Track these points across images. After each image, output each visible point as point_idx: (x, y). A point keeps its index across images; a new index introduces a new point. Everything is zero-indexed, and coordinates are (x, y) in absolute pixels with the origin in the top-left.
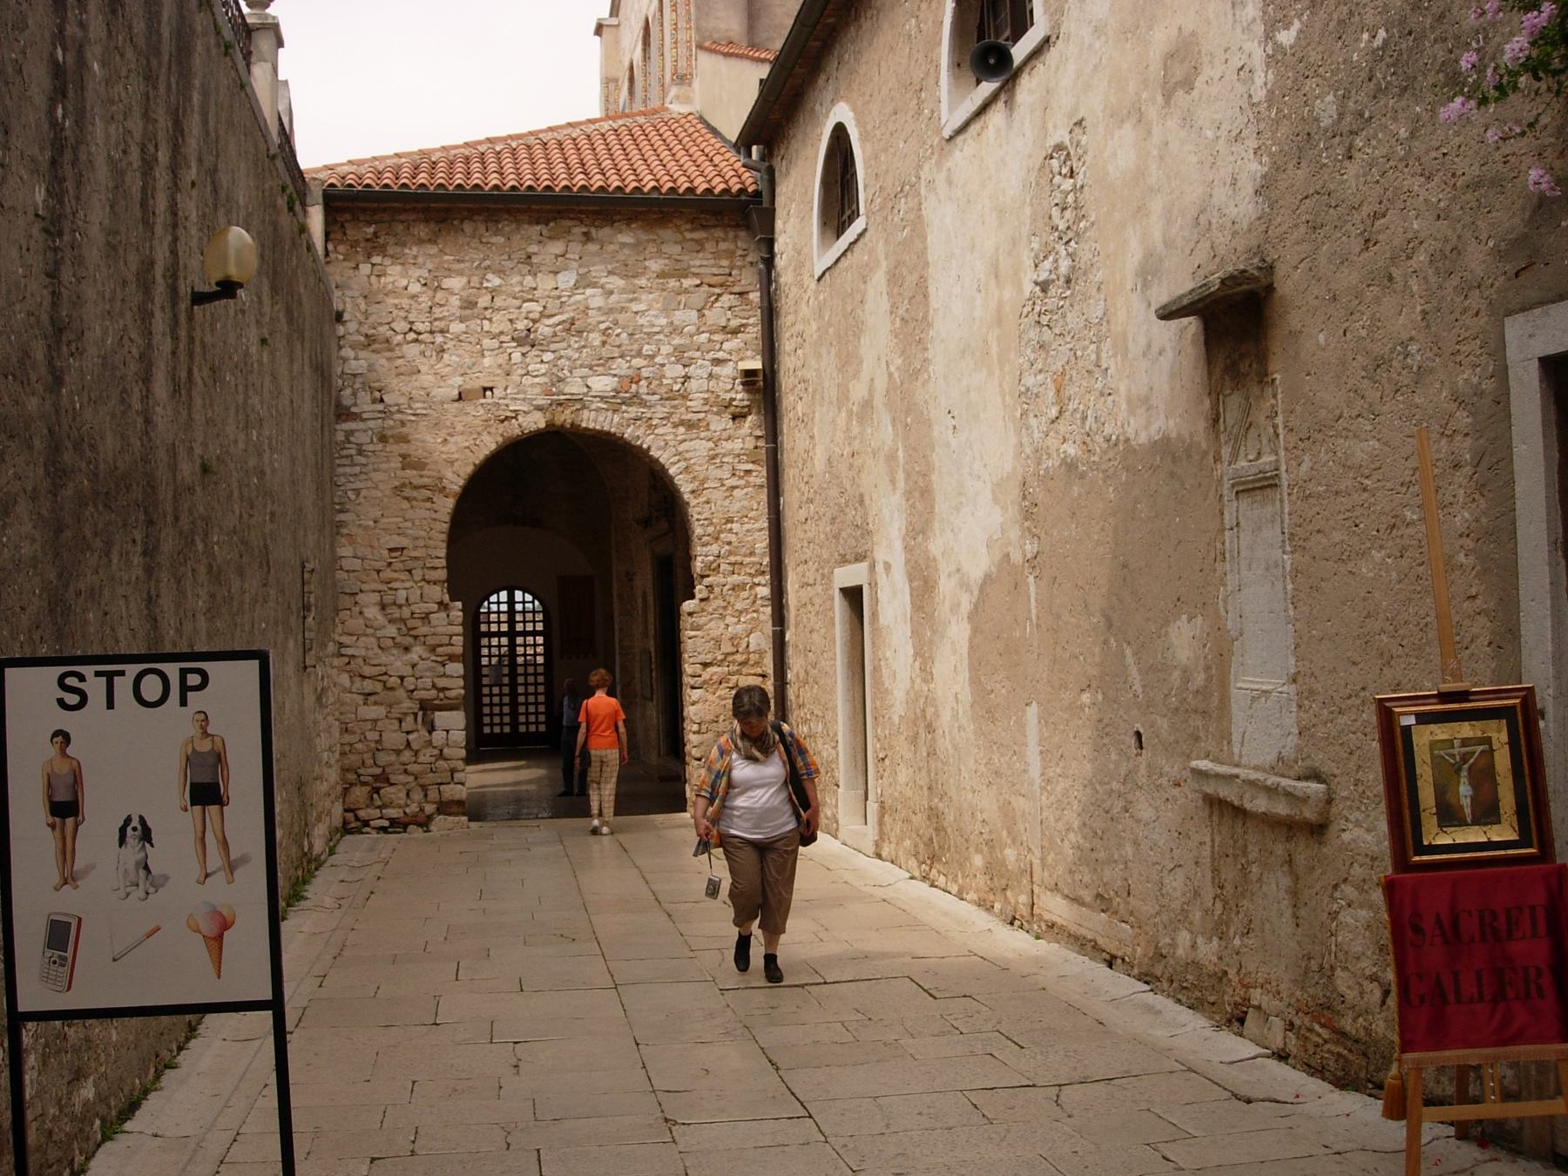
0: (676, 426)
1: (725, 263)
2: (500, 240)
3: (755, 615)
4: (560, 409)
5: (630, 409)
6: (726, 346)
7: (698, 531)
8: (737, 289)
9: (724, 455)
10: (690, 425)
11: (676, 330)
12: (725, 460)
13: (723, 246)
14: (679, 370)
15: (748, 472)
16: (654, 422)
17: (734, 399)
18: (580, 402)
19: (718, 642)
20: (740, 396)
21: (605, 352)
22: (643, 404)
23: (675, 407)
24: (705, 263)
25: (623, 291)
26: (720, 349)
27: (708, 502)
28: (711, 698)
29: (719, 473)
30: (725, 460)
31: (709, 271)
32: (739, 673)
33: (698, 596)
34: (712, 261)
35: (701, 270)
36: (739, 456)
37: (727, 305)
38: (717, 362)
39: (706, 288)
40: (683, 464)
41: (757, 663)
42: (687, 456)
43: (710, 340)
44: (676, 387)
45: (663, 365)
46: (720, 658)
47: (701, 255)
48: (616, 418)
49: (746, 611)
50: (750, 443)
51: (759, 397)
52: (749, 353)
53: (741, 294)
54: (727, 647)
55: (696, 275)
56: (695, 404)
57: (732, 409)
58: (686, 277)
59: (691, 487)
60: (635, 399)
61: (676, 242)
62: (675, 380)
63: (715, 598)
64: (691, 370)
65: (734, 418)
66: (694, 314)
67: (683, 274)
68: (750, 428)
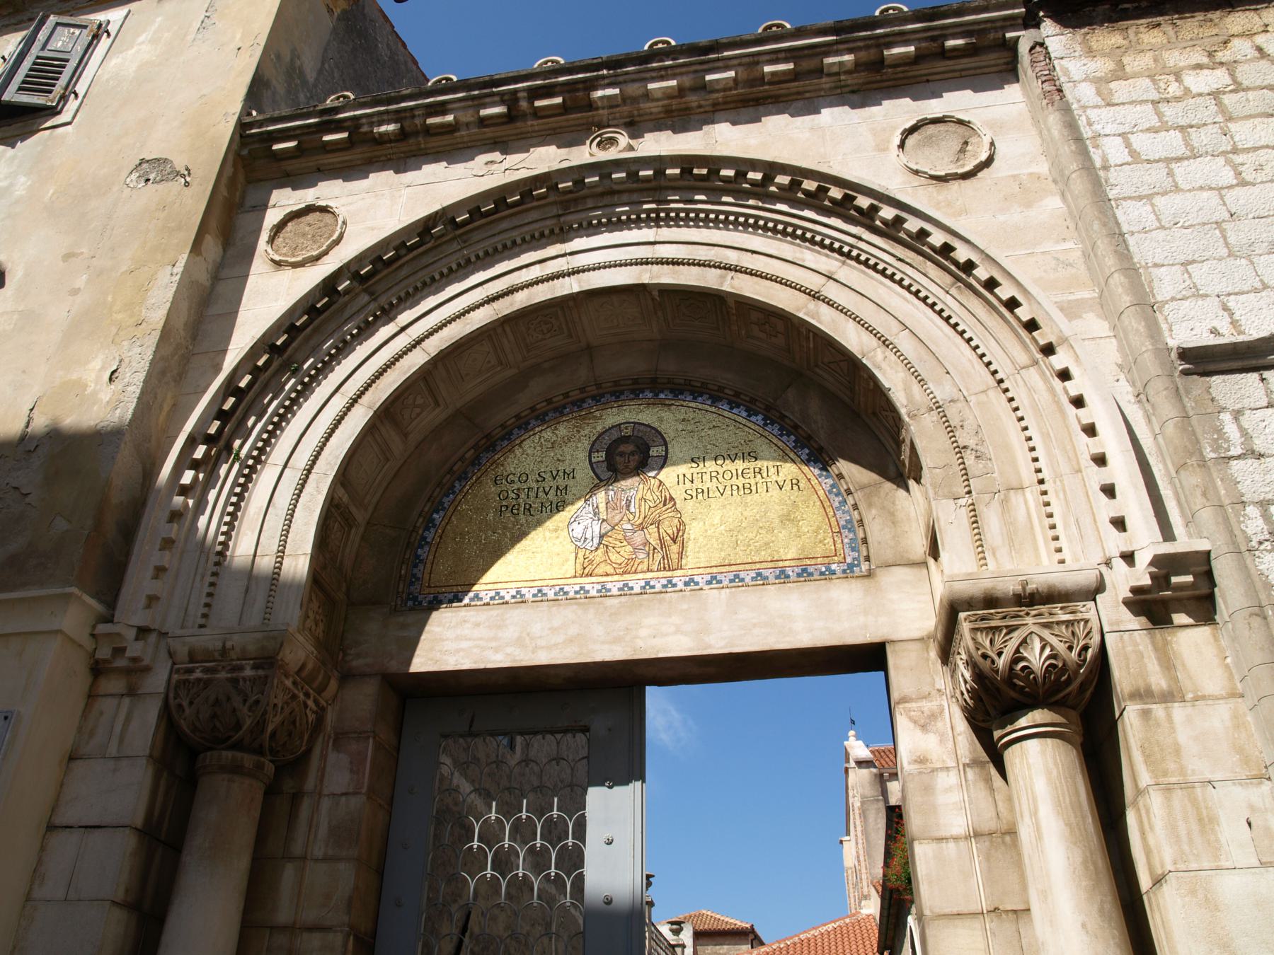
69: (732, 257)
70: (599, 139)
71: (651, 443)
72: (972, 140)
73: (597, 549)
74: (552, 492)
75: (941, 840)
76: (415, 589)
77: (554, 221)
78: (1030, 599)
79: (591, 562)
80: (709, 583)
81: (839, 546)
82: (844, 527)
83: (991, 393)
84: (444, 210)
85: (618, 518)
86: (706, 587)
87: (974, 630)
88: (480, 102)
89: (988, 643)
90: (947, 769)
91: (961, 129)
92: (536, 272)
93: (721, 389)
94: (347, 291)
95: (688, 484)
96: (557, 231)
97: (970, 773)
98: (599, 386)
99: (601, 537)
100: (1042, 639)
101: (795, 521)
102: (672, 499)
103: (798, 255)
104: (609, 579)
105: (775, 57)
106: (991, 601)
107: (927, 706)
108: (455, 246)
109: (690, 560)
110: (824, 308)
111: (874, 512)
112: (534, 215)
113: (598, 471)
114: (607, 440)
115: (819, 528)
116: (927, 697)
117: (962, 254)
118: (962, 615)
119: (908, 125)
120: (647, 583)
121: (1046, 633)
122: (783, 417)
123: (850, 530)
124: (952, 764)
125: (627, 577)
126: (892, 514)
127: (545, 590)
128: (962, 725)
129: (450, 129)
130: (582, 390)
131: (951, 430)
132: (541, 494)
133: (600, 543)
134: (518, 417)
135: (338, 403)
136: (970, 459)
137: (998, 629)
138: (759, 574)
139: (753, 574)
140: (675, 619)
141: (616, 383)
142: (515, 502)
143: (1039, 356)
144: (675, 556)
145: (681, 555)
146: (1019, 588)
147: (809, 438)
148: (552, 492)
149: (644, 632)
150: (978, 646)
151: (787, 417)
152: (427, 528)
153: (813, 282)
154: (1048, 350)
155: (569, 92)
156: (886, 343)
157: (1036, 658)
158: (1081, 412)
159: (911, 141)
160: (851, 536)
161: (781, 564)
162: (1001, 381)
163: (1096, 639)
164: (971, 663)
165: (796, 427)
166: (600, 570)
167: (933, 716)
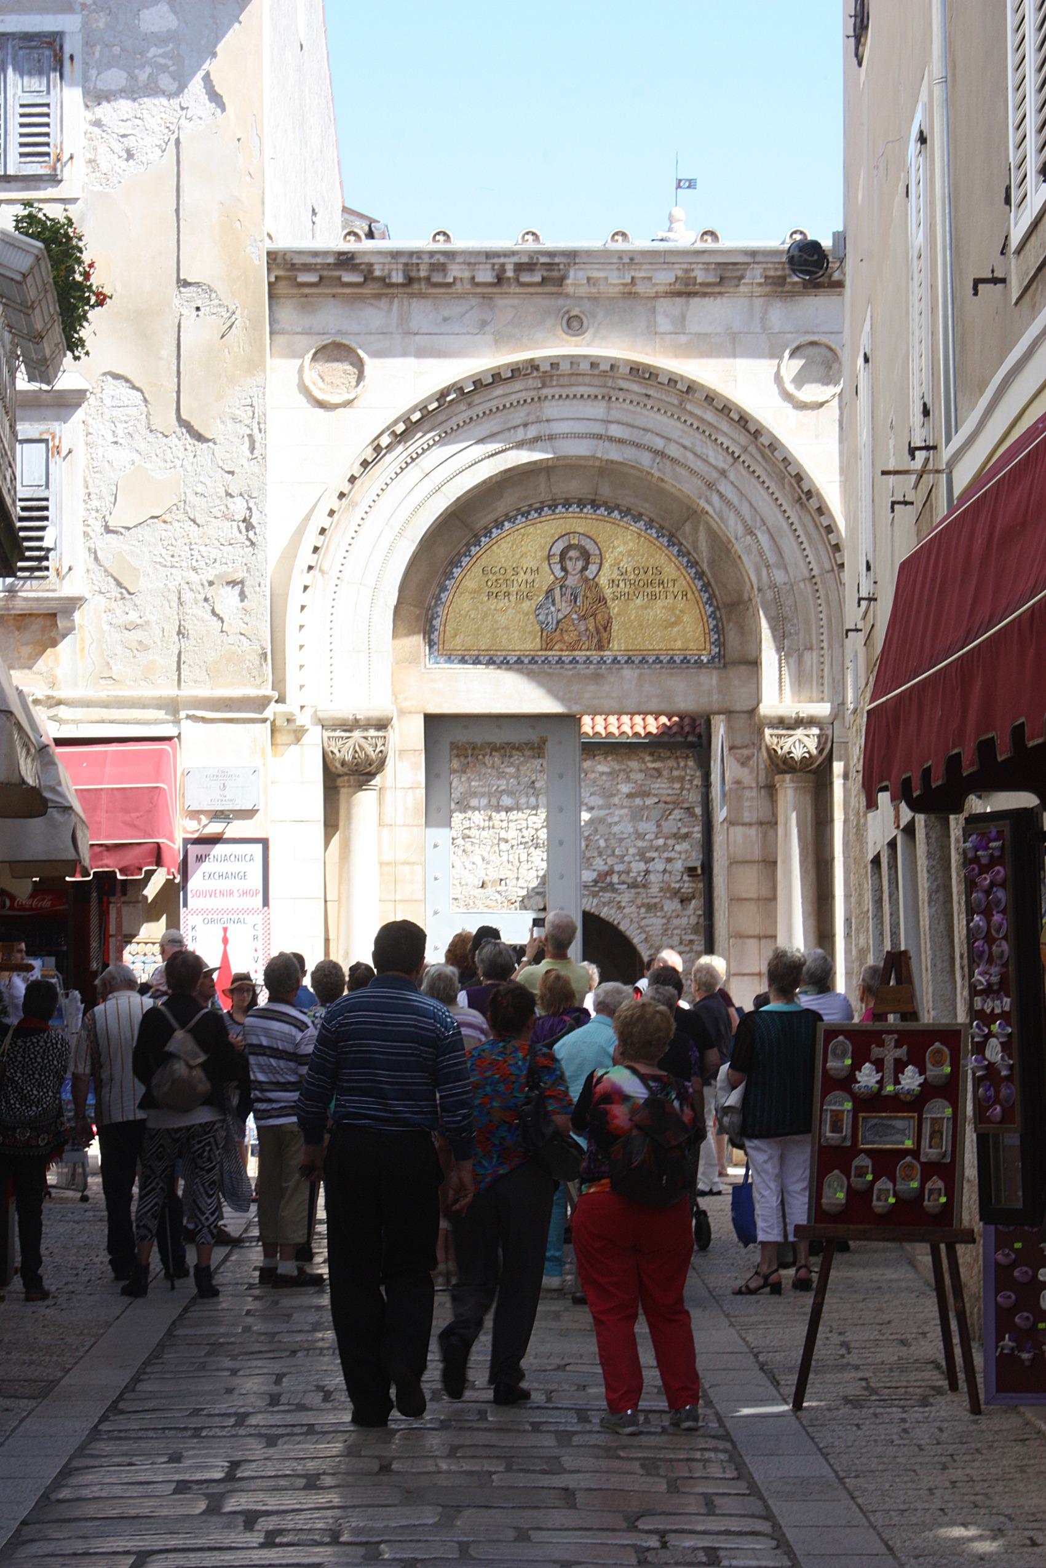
0: (639, 907)
1: (677, 786)
2: (512, 770)
5: (607, 895)
6: (677, 848)
8: (686, 805)
10: (650, 908)
11: (641, 836)
13: (675, 773)
14: (642, 866)
15: (691, 942)
16: (623, 904)
20: (688, 886)
22: (615, 890)
23: (638, 893)
25: (601, 808)
30: (675, 932)
31: (665, 792)
34: (667, 785)
35: (661, 791)
37: (678, 817)
38: (669, 860)
39: (662, 805)
40: (643, 936)
44: (639, 879)
45: (630, 862)
48: (595, 901)
50: (693, 920)
51: (701, 885)
53: (688, 809)
56: (654, 890)
60: (611, 887)
61: (641, 771)
62: (639, 872)
65: (682, 901)
67: (645, 794)
68: (695, 910)
69: (659, 444)
71: (591, 552)
72: (835, 366)
79: (551, 640)
85: (569, 609)
87: (771, 736)
91: (829, 355)
93: (641, 515)
95: (615, 588)
96: (536, 399)
97: (763, 791)
99: (558, 622)
102: (604, 598)
103: (704, 451)
104: (564, 653)
107: (746, 752)
108: (463, 407)
109: (615, 645)
111: (731, 625)
112: (518, 385)
116: (746, 747)
121: (805, 739)
124: (754, 785)
125: (576, 653)
126: (742, 627)
127: (523, 658)
129: (449, 285)
130: (542, 502)
134: (496, 520)
138: (657, 658)
140: (606, 688)
141: (567, 499)
143: (835, 568)
147: (697, 563)
149: (587, 695)
151: (681, 544)
152: (436, 605)
155: (547, 270)
161: (671, 652)
162: (814, 577)
163: (829, 745)
165: (689, 553)
167: (749, 758)
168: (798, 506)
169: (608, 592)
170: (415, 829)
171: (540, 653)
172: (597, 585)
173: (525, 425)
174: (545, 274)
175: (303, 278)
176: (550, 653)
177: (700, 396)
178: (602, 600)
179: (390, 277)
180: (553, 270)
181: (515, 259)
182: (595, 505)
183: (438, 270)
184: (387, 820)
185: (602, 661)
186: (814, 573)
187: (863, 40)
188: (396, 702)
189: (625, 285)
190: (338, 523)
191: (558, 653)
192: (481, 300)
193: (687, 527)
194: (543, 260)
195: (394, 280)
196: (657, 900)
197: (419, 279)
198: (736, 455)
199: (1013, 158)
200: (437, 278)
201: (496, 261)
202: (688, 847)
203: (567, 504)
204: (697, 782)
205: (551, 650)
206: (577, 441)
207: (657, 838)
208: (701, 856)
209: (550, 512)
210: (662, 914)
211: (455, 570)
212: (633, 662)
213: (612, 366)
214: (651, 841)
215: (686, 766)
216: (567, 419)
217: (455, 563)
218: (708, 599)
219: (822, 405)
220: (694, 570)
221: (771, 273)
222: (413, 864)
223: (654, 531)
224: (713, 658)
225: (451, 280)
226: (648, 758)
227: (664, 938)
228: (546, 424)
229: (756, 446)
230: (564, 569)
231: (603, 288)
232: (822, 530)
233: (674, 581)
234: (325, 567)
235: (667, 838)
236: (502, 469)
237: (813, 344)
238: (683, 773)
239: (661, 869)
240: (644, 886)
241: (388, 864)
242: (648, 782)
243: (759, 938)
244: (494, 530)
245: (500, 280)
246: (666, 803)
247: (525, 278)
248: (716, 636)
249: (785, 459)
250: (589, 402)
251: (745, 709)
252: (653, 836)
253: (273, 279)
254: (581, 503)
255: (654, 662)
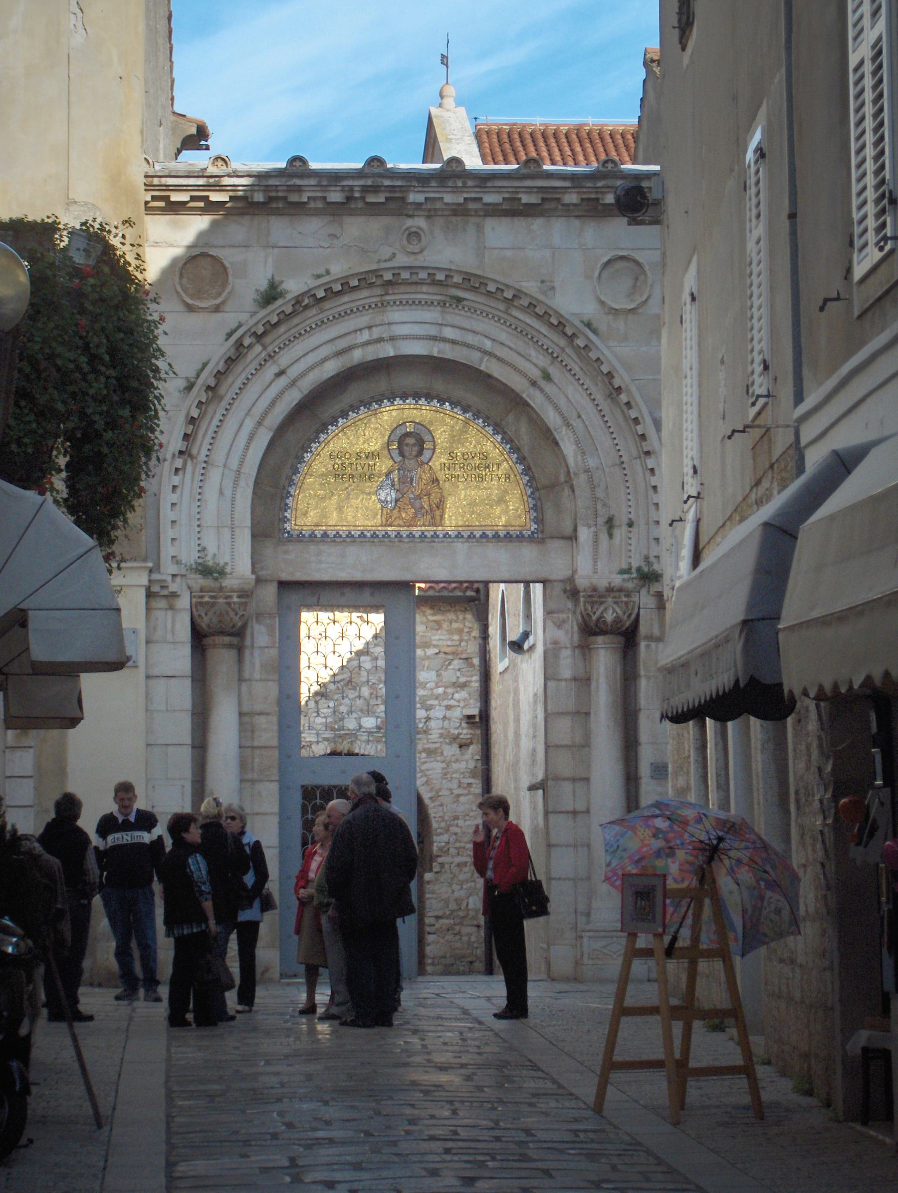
1: (456, 637)
3: (473, 884)
4: (340, 740)
6: (456, 696)
7: (435, 825)
8: (464, 656)
9: (453, 773)
12: (454, 776)
13: (455, 625)
15: (469, 784)
17: (461, 734)
18: (353, 736)
19: (447, 902)
20: (466, 732)
21: (373, 702)
24: (442, 637)
26: (452, 698)
27: (441, 805)
28: (442, 941)
29: (450, 785)
30: (454, 776)
31: (445, 643)
32: (461, 924)
33: (434, 870)
34: (448, 637)
35: (440, 643)
36: (463, 773)
37: (458, 667)
38: (449, 708)
39: (442, 655)
40: (424, 779)
41: (474, 918)
42: (428, 773)
43: (445, 692)
46: (448, 913)
47: (439, 632)
49: (467, 881)
50: (472, 764)
51: (478, 732)
52: (472, 701)
54: (453, 906)
55: (435, 646)
56: (434, 736)
57: (458, 741)
58: (429, 647)
59: (430, 795)
63: (446, 872)
64: (432, 714)
65: (461, 747)
66: (434, 673)
68: (472, 754)
69: (488, 345)
70: (407, 232)
72: (642, 278)
73: (394, 508)
74: (366, 467)
75: (559, 680)
76: (287, 526)
77: (378, 299)
78: (610, 590)
79: (391, 517)
80: (457, 537)
81: (528, 520)
82: (532, 509)
83: (617, 468)
84: (310, 290)
85: (406, 490)
86: (455, 540)
87: (585, 602)
88: (324, 188)
89: (590, 608)
90: (566, 648)
92: (365, 336)
94: (249, 346)
96: (380, 305)
97: (577, 650)
98: (393, 393)
99: (396, 501)
100: (613, 609)
101: (506, 502)
102: (437, 480)
105: (529, 190)
106: (595, 589)
107: (563, 616)
108: (314, 311)
110: (537, 394)
112: (365, 293)
113: (393, 455)
114: (399, 433)
115: (518, 508)
116: (562, 612)
117: (617, 382)
118: (581, 594)
119: (605, 259)
120: (423, 533)
121: (615, 606)
122: (505, 433)
123: (535, 511)
124: (569, 645)
128: (576, 628)
131: (593, 488)
132: (359, 468)
133: (396, 505)
134: (342, 411)
135: (249, 424)
136: (599, 506)
137: (596, 602)
138: (484, 533)
139: (481, 533)
142: (343, 472)
143: (642, 455)
144: (438, 518)
145: (442, 517)
146: (607, 585)
148: (366, 467)
150: (586, 610)
152: (290, 486)
153: (535, 373)
154: (648, 453)
155: (390, 192)
156: (568, 425)
157: (609, 617)
158: (654, 496)
159: (605, 274)
160: (535, 514)
161: (496, 528)
163: (636, 610)
164: (581, 613)
165: (512, 441)
166: (396, 523)
167: (564, 621)
168: (609, 400)
169: (441, 476)
170: (270, 683)
171: (380, 528)
172: (431, 467)
173: (370, 328)
174: (388, 195)
175: (175, 197)
176: (389, 528)
177: (525, 302)
178: (436, 481)
179: (252, 198)
180: (395, 192)
181: (361, 182)
182: (429, 397)
183: (295, 191)
184: (246, 675)
185: (435, 536)
186: (623, 459)
187: (687, 32)
188: (253, 572)
189: (459, 204)
190: (205, 413)
191: (396, 528)
192: (331, 218)
193: (511, 418)
194: (387, 183)
195: (256, 200)
196: (438, 745)
197: (277, 199)
198: (555, 355)
199: (856, 216)
200: (293, 198)
201: (345, 183)
202: (467, 695)
203: (404, 397)
204: (476, 633)
205: (390, 525)
206: (416, 341)
207: (437, 687)
208: (479, 704)
209: (389, 404)
210: (443, 758)
211: (305, 455)
212: (462, 537)
213: (447, 276)
214: (432, 689)
215: (464, 619)
216: (406, 323)
217: (306, 449)
218: (528, 481)
219: (632, 311)
220: (516, 455)
221: (584, 196)
222: (268, 714)
223: (481, 421)
224: (533, 533)
225: (306, 200)
226: (429, 612)
227: (444, 781)
228: (386, 327)
229: (573, 346)
230: (402, 454)
231: (438, 205)
232: (631, 422)
233: (499, 465)
234: (194, 452)
235: (446, 687)
236: (349, 365)
237: (622, 258)
238: (461, 626)
239: (441, 717)
240: (425, 732)
241: (246, 714)
242: (429, 634)
243: (574, 780)
244: (340, 420)
245: (349, 199)
246: (445, 653)
247: (371, 199)
248: (535, 514)
249: (598, 359)
250: (426, 307)
251: (560, 578)
252: (432, 685)
253: (149, 199)
254: (417, 396)
255: (481, 536)
